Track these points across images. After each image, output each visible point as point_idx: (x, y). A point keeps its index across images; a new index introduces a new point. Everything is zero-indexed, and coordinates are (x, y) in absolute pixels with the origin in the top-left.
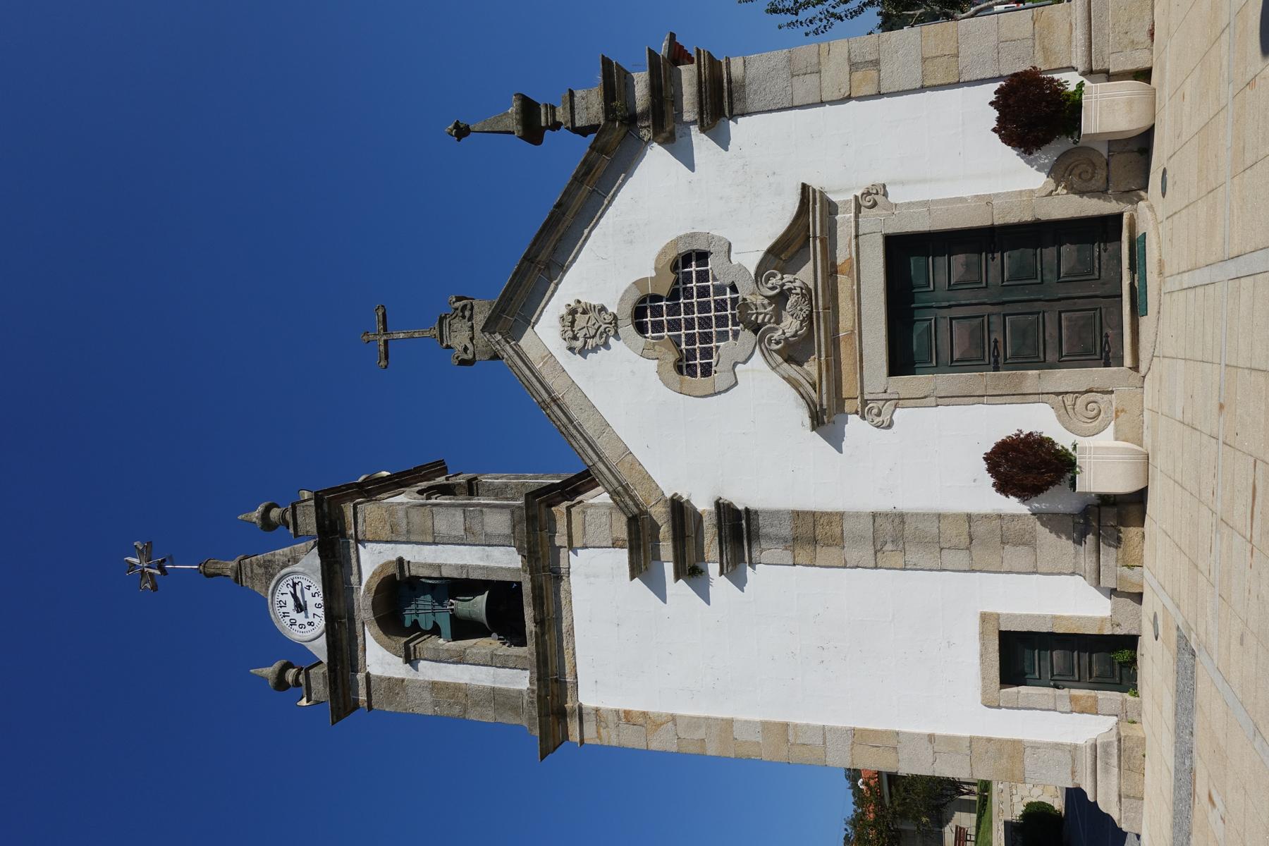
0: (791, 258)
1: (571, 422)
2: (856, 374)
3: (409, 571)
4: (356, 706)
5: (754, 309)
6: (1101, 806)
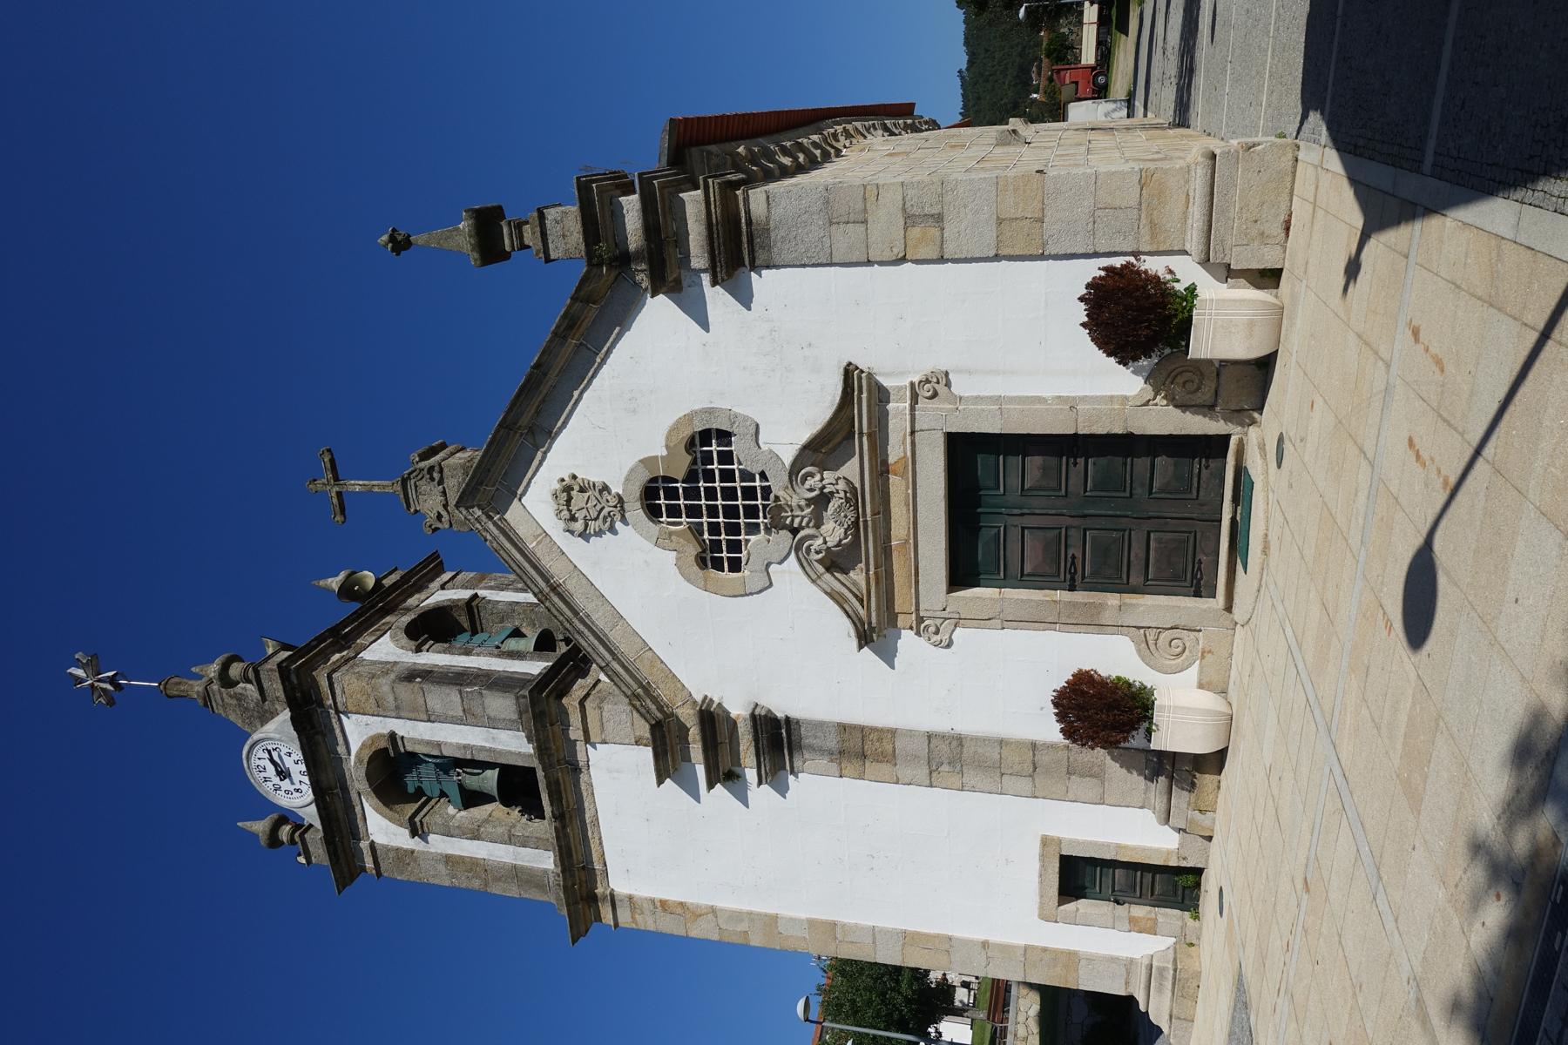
0: (833, 450)
1: (576, 613)
2: (911, 588)
3: (404, 747)
4: (363, 869)
5: (788, 510)
6: (1151, 1018)
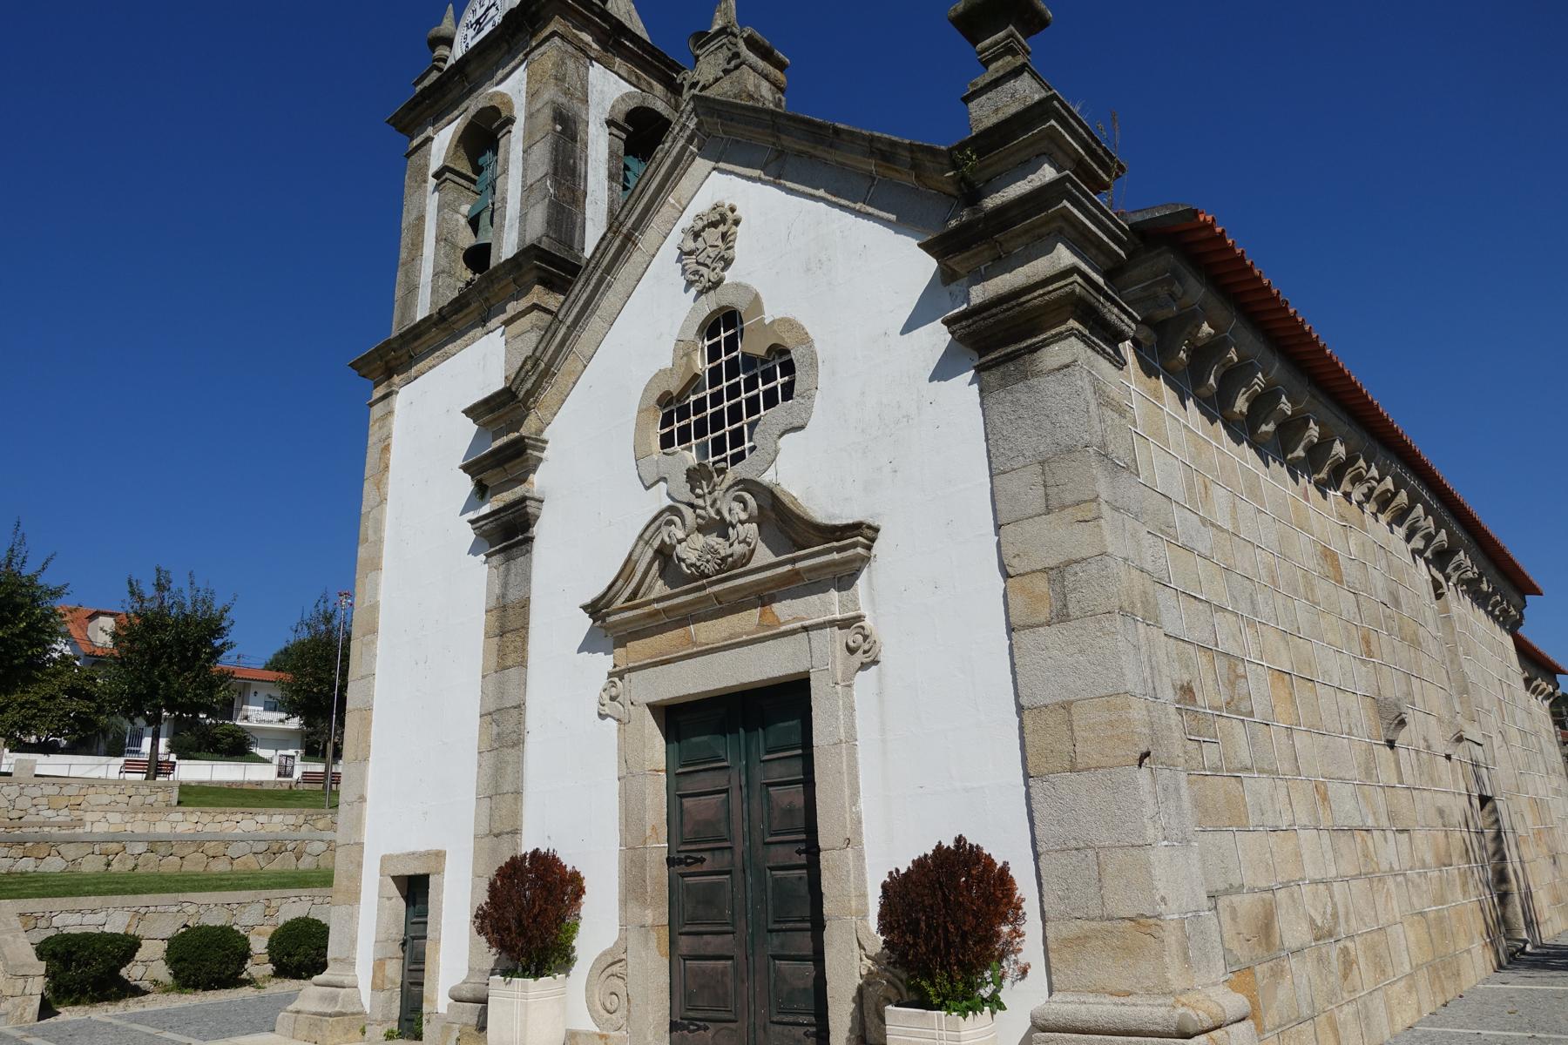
1: (608, 270)
2: (651, 658)
4: (412, 139)
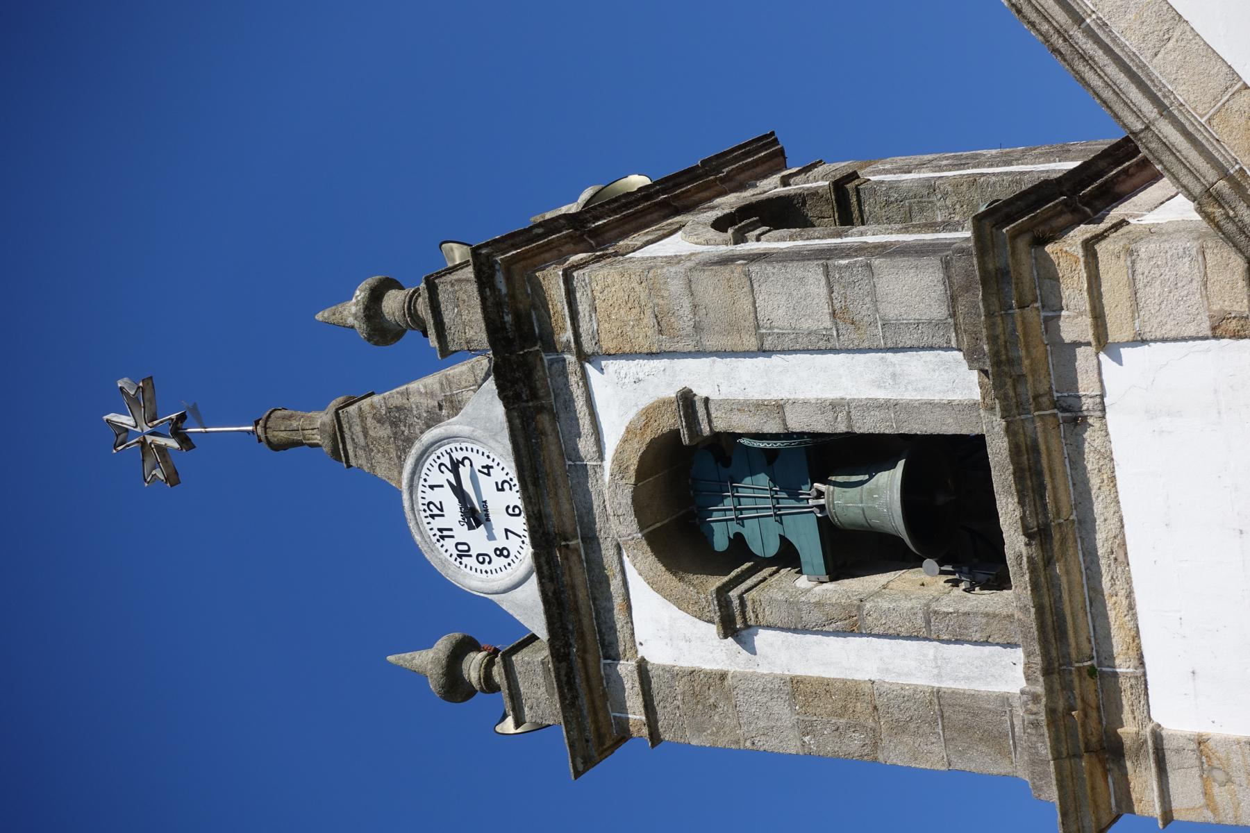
1: (1079, 20)
3: (710, 422)
4: (624, 734)
